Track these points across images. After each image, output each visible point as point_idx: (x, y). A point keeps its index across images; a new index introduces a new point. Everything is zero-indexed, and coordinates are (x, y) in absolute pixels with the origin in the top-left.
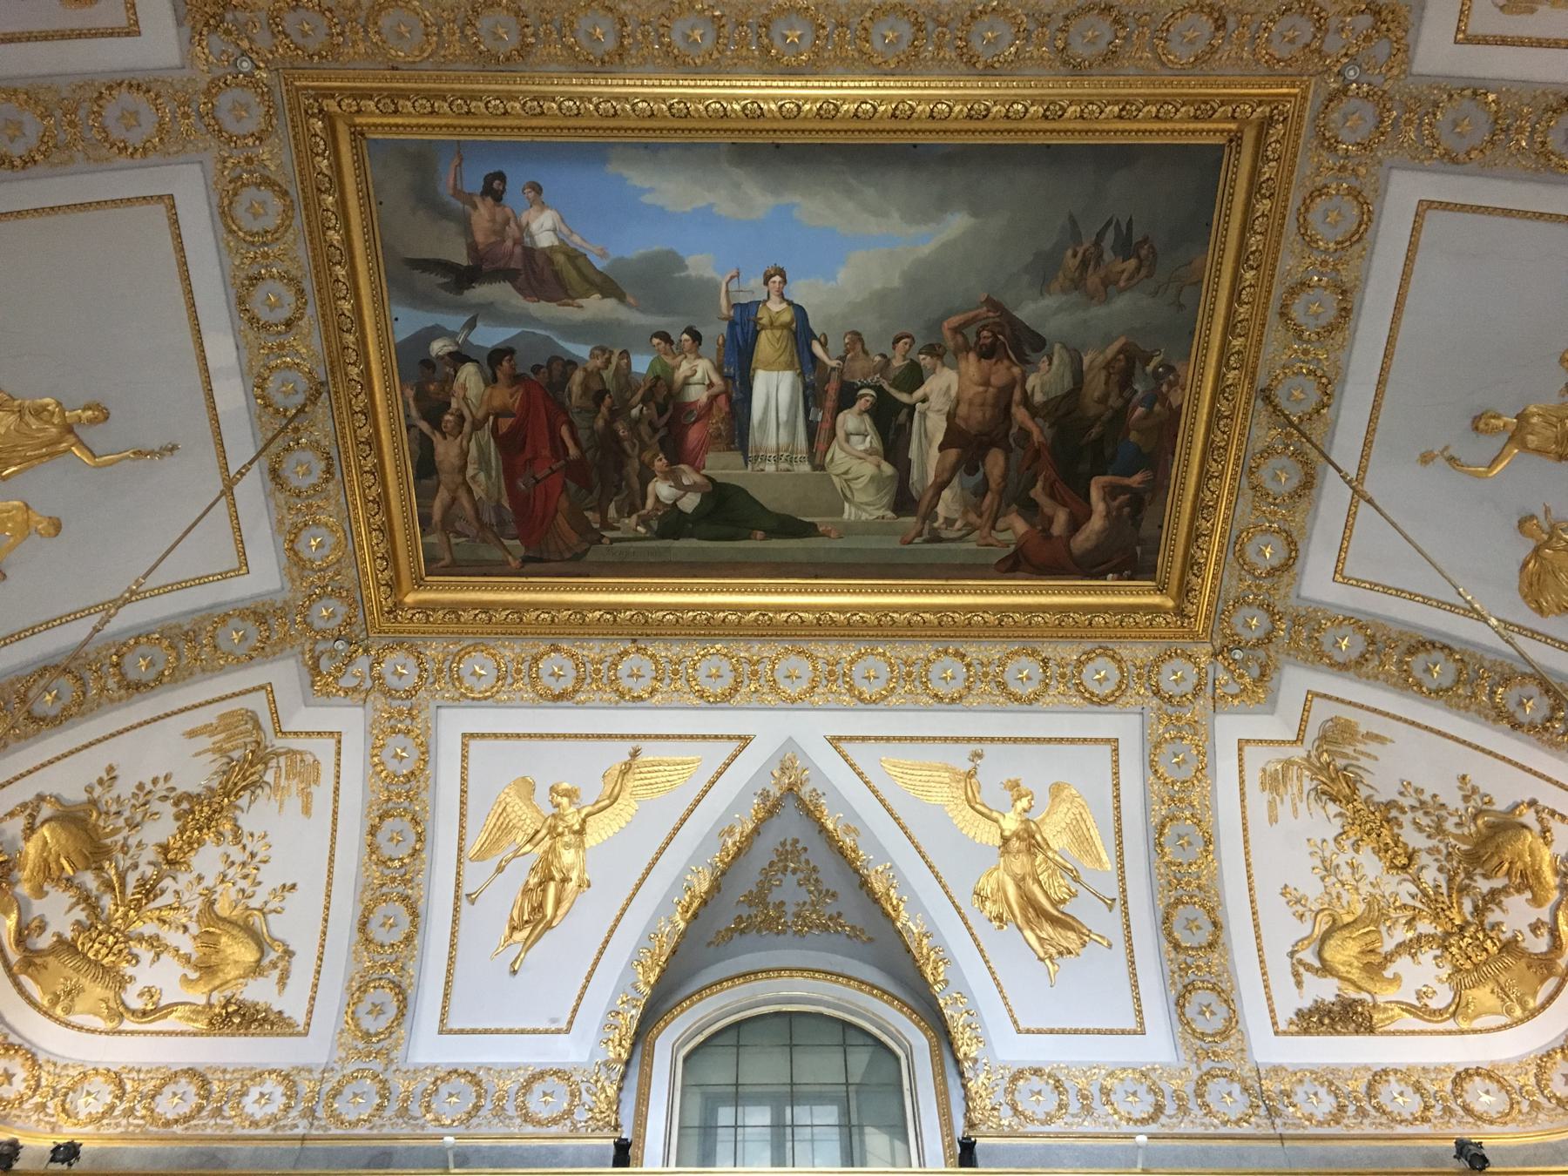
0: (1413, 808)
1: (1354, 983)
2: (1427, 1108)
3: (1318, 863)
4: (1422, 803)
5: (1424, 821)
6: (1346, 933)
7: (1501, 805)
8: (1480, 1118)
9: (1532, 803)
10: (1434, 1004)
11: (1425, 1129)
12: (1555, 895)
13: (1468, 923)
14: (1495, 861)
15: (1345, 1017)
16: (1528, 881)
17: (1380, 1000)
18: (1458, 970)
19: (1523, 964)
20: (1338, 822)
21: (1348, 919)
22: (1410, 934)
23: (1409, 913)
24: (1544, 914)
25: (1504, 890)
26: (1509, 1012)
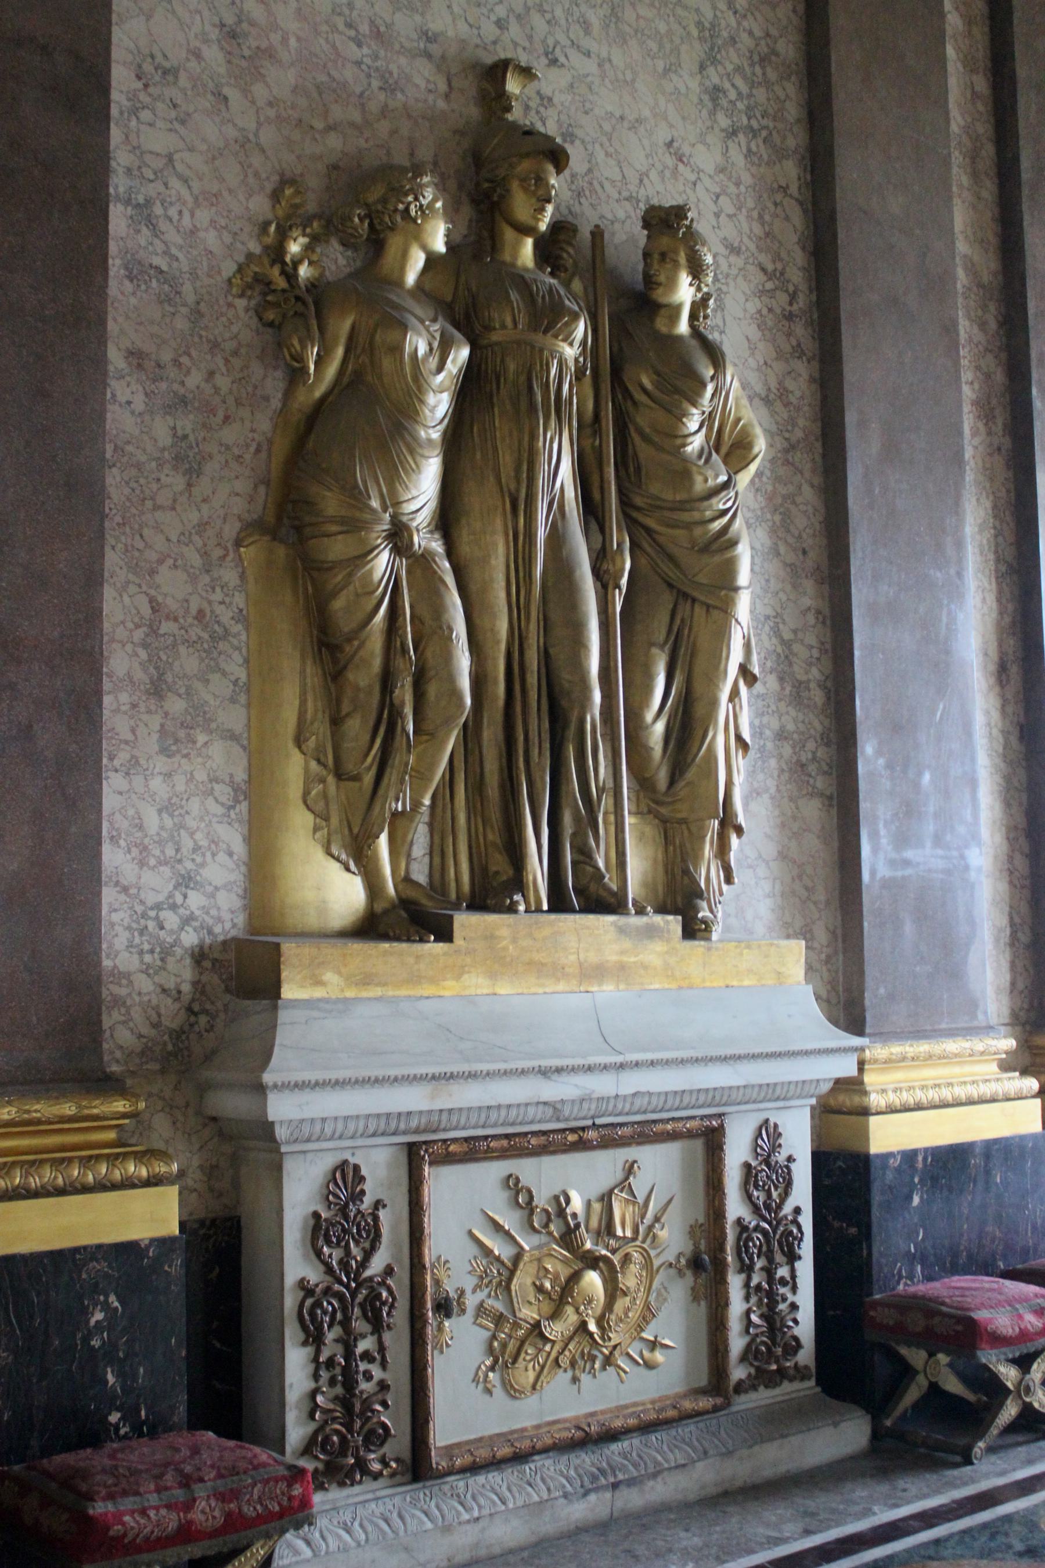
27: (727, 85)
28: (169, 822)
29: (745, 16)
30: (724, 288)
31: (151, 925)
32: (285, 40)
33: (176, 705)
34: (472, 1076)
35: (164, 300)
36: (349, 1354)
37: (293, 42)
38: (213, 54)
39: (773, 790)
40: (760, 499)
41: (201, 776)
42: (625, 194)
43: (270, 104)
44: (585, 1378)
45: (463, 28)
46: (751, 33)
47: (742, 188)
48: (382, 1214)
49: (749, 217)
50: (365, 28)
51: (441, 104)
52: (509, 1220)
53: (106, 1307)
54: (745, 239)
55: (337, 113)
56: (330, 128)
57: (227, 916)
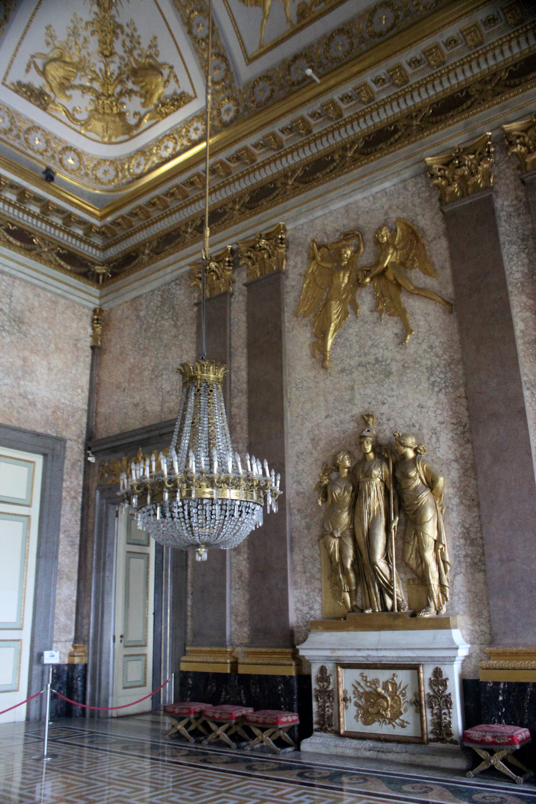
0: (128, 35)
1: (51, 86)
2: (46, 151)
3: (72, 26)
4: (133, 35)
5: (128, 43)
6: (62, 65)
7: (160, 60)
8: (63, 166)
9: (171, 67)
10: (77, 116)
11: (39, 157)
12: (152, 107)
13: (113, 95)
14: (141, 79)
15: (38, 97)
16: (147, 95)
17: (57, 100)
18: (96, 110)
19: (121, 124)
20: (93, 16)
21: (68, 60)
22: (88, 84)
23: (94, 76)
24: (143, 111)
25: (136, 93)
26: (103, 137)
33: (308, 575)
34: (339, 649)
35: (303, 497)
38: (310, 446)
45: (361, 410)
49: (447, 411)
52: (362, 684)
55: (334, 444)
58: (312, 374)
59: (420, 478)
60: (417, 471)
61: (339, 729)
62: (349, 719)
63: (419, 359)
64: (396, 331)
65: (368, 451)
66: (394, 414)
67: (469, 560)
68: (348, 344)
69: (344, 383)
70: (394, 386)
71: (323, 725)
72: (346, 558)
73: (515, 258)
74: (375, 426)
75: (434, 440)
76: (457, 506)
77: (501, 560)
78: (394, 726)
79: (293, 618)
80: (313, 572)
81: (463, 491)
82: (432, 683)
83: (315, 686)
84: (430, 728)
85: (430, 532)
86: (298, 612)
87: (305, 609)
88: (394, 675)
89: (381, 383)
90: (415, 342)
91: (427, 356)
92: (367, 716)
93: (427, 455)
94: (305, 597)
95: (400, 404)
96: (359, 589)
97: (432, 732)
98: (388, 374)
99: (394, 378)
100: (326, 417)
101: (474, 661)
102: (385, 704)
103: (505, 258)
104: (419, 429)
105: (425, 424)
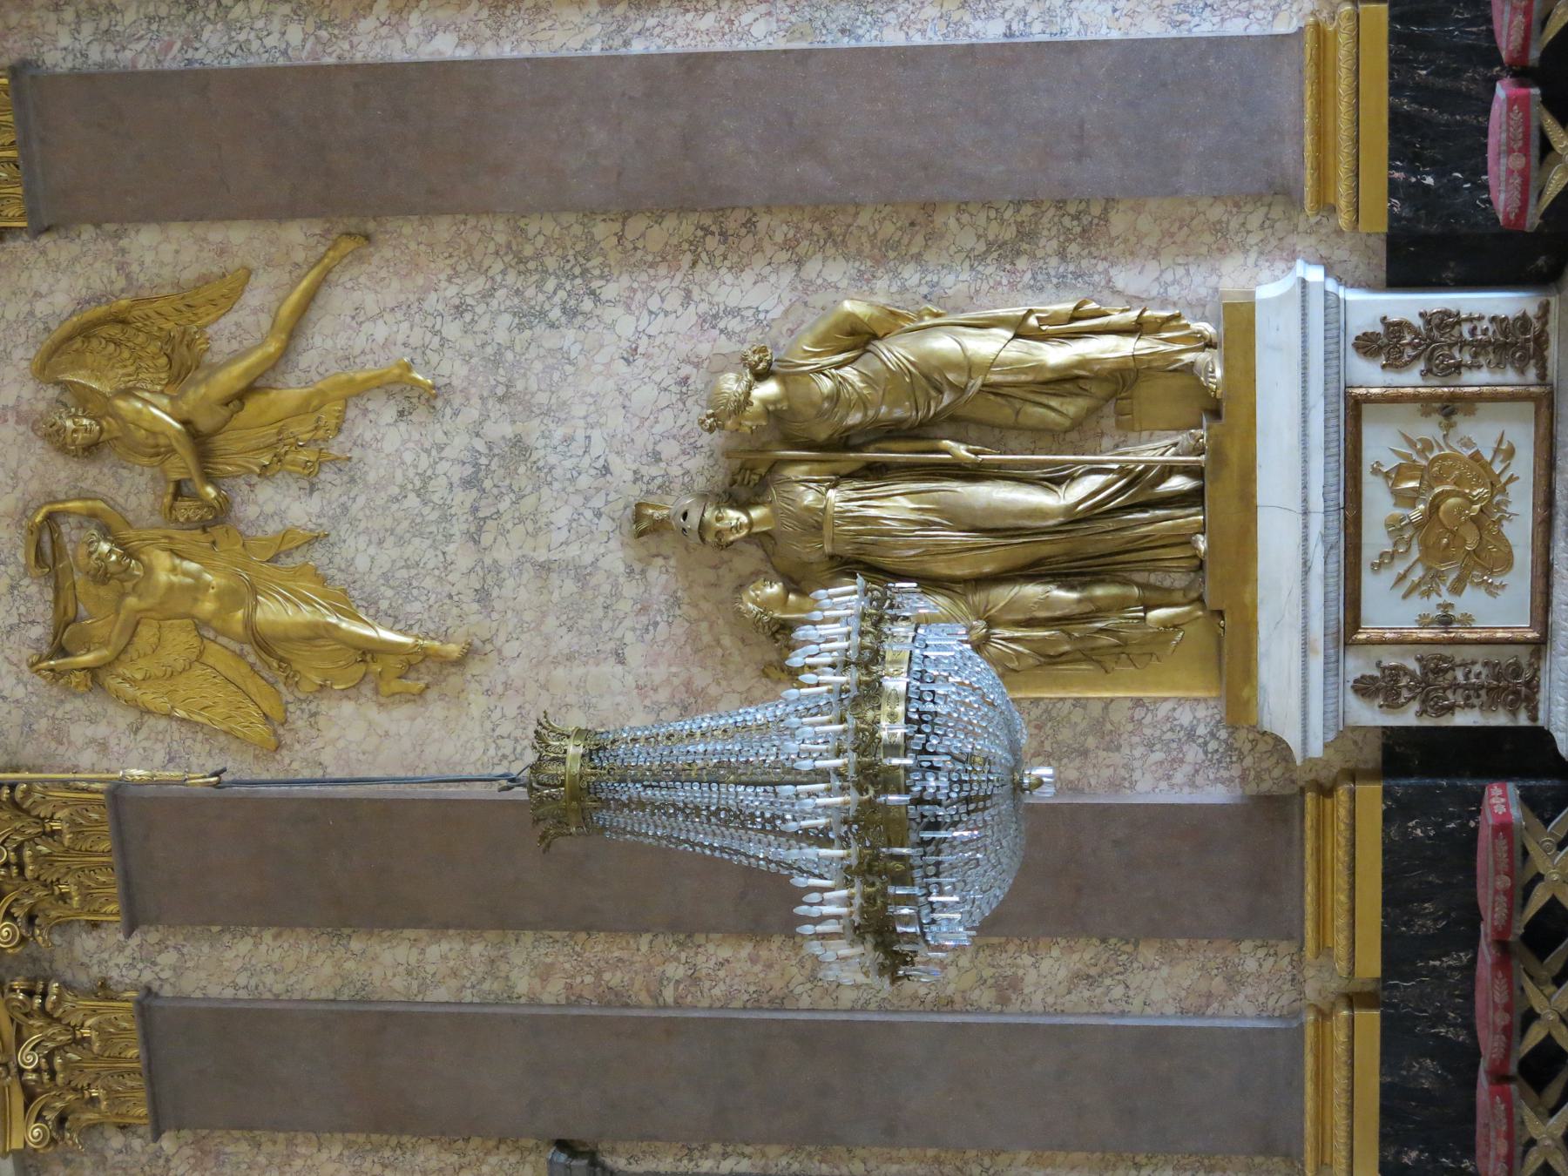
27: (557, 299)
28: (1158, 746)
29: (492, 279)
30: (722, 307)
31: (1216, 756)
32: (675, 675)
33: (1091, 742)
36: (1464, 687)
37: (674, 669)
39: (1106, 264)
40: (879, 274)
41: (1130, 727)
42: (681, 405)
43: (719, 684)
44: (1511, 509)
45: (614, 544)
46: (504, 272)
47: (635, 285)
48: (1385, 664)
49: (655, 278)
50: (644, 619)
51: (672, 562)
52: (1400, 567)
53: (1414, 828)
54: (675, 283)
55: (707, 639)
56: (718, 642)
57: (1210, 712)
58: (477, 703)
59: (839, 366)
60: (820, 371)
61: (1526, 642)
62: (1498, 610)
63: (489, 350)
64: (389, 413)
65: (744, 519)
66: (641, 438)
67: (1073, 248)
68: (404, 573)
69: (523, 595)
70: (559, 433)
71: (1516, 693)
72: (1046, 603)
73: (242, 37)
74: (670, 500)
75: (733, 324)
76: (925, 271)
77: (1079, 157)
78: (1511, 479)
79: (1216, 794)
80: (1083, 725)
81: (886, 253)
82: (1395, 363)
83: (1408, 717)
84: (1511, 376)
85: (989, 345)
86: (1199, 780)
87: (1193, 754)
88: (1375, 471)
89: (542, 476)
90: (434, 358)
91: (484, 324)
92: (1487, 560)
93: (775, 346)
94: (1159, 756)
95: (615, 420)
96: (1138, 577)
97: (1522, 371)
98: (519, 447)
99: (532, 430)
100: (621, 660)
101: (1340, 254)
102: (1452, 501)
103: (234, 63)
104: (697, 365)
105: (684, 348)
